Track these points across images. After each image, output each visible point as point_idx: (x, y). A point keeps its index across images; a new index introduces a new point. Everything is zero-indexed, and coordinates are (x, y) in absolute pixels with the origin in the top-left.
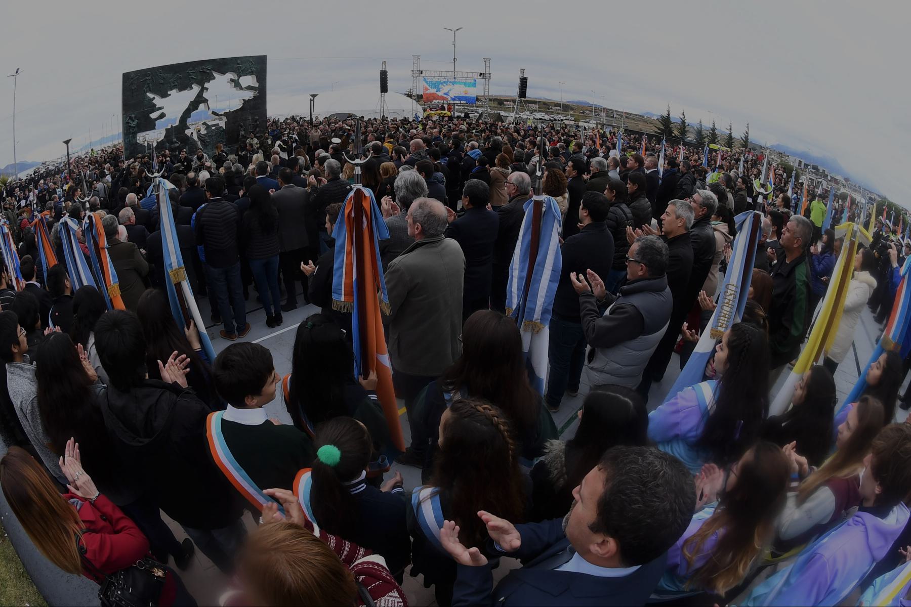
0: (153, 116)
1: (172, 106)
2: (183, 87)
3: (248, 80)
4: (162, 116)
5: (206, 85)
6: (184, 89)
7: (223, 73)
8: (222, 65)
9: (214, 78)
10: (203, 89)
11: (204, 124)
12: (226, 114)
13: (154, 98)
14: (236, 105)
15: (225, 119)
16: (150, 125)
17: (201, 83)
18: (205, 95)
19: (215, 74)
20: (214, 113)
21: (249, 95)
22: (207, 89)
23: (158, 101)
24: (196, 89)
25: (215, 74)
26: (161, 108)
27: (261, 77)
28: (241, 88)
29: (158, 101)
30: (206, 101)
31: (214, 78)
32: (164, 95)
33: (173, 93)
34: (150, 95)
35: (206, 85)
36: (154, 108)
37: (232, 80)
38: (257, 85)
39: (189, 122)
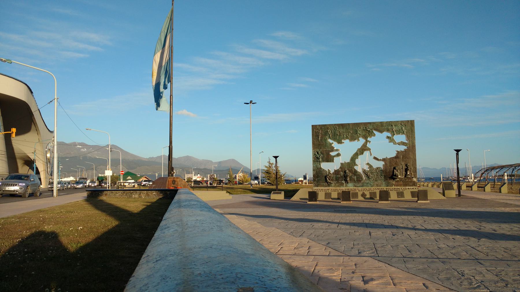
0: (333, 154)
1: (345, 150)
2: (353, 139)
3: (401, 138)
4: (338, 155)
6: (355, 140)
7: (381, 132)
8: (381, 127)
9: (374, 135)
10: (367, 141)
11: (368, 164)
12: (384, 160)
13: (333, 143)
15: (383, 163)
16: (330, 159)
17: (365, 137)
18: (368, 145)
19: (374, 132)
20: (375, 158)
23: (335, 145)
24: (362, 141)
25: (374, 132)
28: (395, 143)
29: (335, 145)
30: (369, 149)
31: (374, 135)
32: (340, 142)
33: (346, 142)
34: (330, 141)
35: (369, 139)
36: (332, 149)
37: (388, 137)
39: (357, 161)
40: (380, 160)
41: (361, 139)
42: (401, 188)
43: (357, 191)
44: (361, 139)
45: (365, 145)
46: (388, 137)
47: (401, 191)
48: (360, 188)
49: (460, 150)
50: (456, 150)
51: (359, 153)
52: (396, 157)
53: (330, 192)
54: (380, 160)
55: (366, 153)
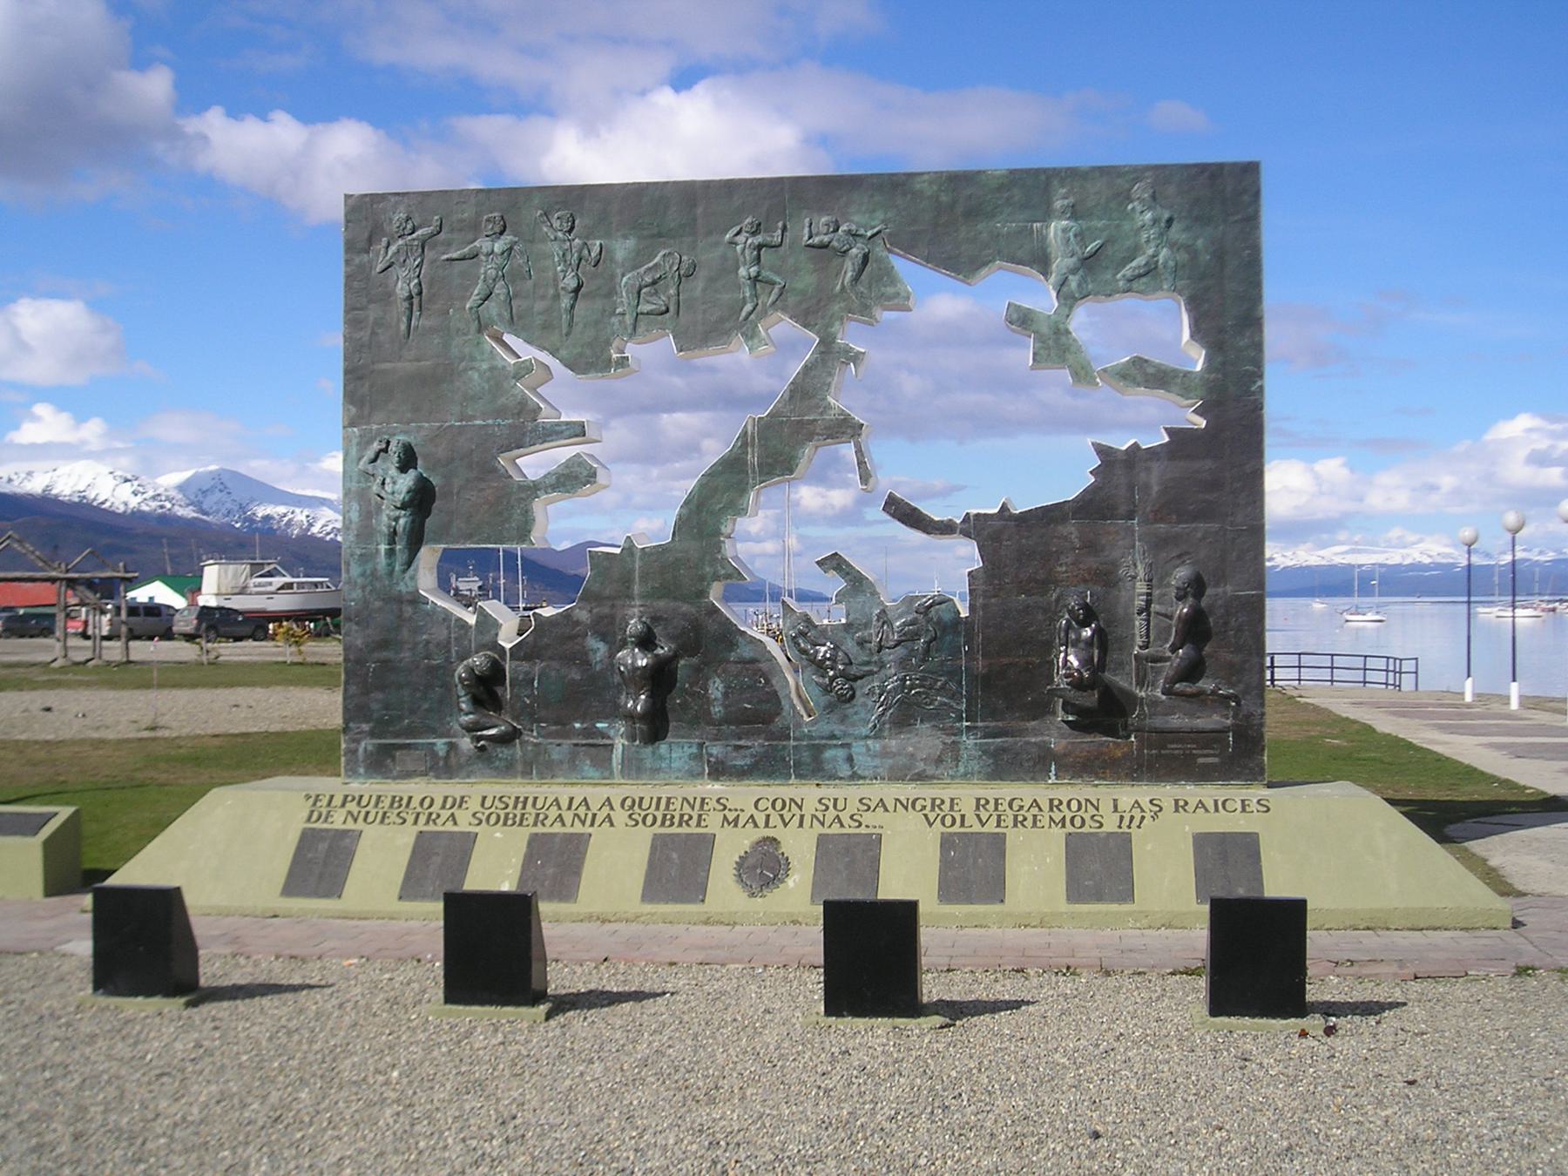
7: (962, 264)
8: (960, 218)
10: (830, 354)
12: (974, 527)
14: (1054, 473)
15: (966, 556)
19: (907, 269)
21: (1150, 420)
23: (562, 394)
26: (578, 431)
27: (1229, 309)
32: (592, 359)
33: (651, 352)
37: (1022, 320)
40: (946, 528)
42: (1114, 802)
43: (713, 822)
44: (782, 327)
47: (1110, 825)
48: (743, 795)
51: (752, 457)
52: (1090, 507)
53: (465, 824)
54: (946, 528)
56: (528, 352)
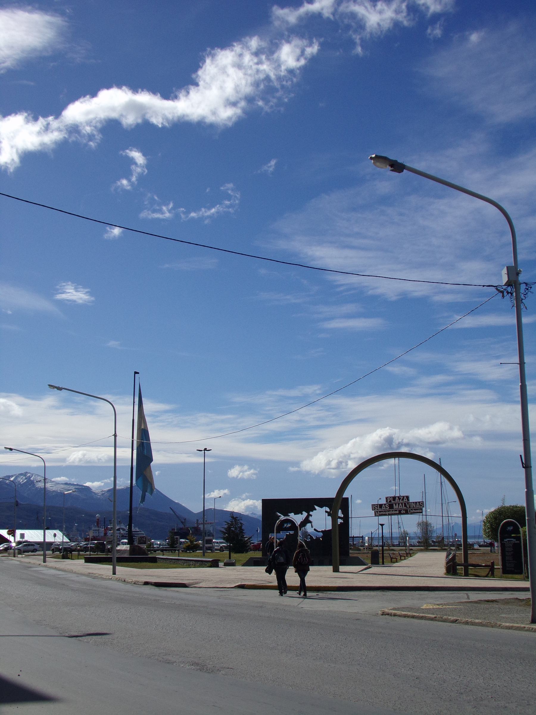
5: (311, 513)
6: (298, 514)
7: (321, 507)
9: (315, 509)
10: (309, 515)
12: (322, 531)
15: (321, 534)
17: (308, 512)
18: (311, 519)
19: (316, 507)
20: (315, 530)
22: (311, 515)
24: (305, 514)
25: (316, 507)
30: (311, 522)
31: (315, 509)
35: (311, 513)
37: (326, 512)
38: (342, 516)
40: (320, 532)
41: (304, 512)
44: (304, 512)
45: (307, 517)
46: (326, 512)
49: (383, 525)
50: (381, 524)
55: (309, 525)
56: (279, 514)
